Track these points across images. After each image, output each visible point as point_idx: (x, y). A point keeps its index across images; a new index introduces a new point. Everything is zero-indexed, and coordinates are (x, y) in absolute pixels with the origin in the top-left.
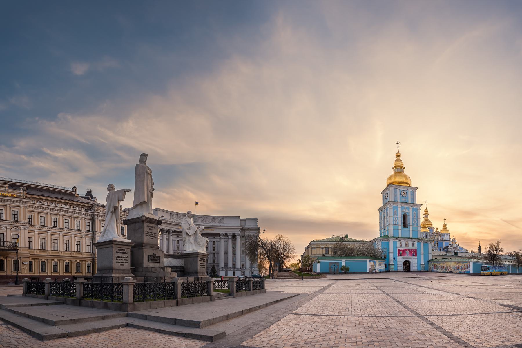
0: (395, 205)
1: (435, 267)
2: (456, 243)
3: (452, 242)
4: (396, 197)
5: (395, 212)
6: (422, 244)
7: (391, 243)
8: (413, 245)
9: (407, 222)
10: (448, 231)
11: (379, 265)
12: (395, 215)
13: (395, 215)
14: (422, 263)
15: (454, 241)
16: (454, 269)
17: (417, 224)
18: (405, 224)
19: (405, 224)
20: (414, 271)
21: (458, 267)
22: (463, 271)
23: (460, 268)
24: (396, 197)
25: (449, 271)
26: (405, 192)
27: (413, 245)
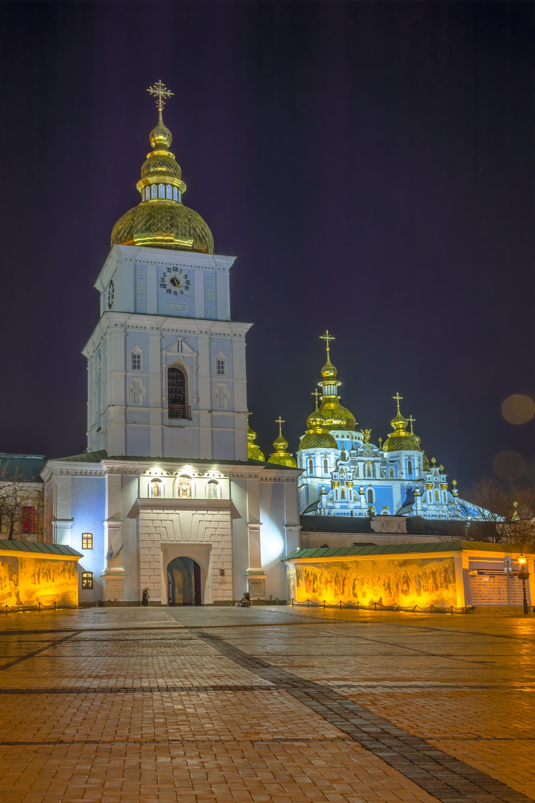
13: (136, 365)
26: (180, 278)
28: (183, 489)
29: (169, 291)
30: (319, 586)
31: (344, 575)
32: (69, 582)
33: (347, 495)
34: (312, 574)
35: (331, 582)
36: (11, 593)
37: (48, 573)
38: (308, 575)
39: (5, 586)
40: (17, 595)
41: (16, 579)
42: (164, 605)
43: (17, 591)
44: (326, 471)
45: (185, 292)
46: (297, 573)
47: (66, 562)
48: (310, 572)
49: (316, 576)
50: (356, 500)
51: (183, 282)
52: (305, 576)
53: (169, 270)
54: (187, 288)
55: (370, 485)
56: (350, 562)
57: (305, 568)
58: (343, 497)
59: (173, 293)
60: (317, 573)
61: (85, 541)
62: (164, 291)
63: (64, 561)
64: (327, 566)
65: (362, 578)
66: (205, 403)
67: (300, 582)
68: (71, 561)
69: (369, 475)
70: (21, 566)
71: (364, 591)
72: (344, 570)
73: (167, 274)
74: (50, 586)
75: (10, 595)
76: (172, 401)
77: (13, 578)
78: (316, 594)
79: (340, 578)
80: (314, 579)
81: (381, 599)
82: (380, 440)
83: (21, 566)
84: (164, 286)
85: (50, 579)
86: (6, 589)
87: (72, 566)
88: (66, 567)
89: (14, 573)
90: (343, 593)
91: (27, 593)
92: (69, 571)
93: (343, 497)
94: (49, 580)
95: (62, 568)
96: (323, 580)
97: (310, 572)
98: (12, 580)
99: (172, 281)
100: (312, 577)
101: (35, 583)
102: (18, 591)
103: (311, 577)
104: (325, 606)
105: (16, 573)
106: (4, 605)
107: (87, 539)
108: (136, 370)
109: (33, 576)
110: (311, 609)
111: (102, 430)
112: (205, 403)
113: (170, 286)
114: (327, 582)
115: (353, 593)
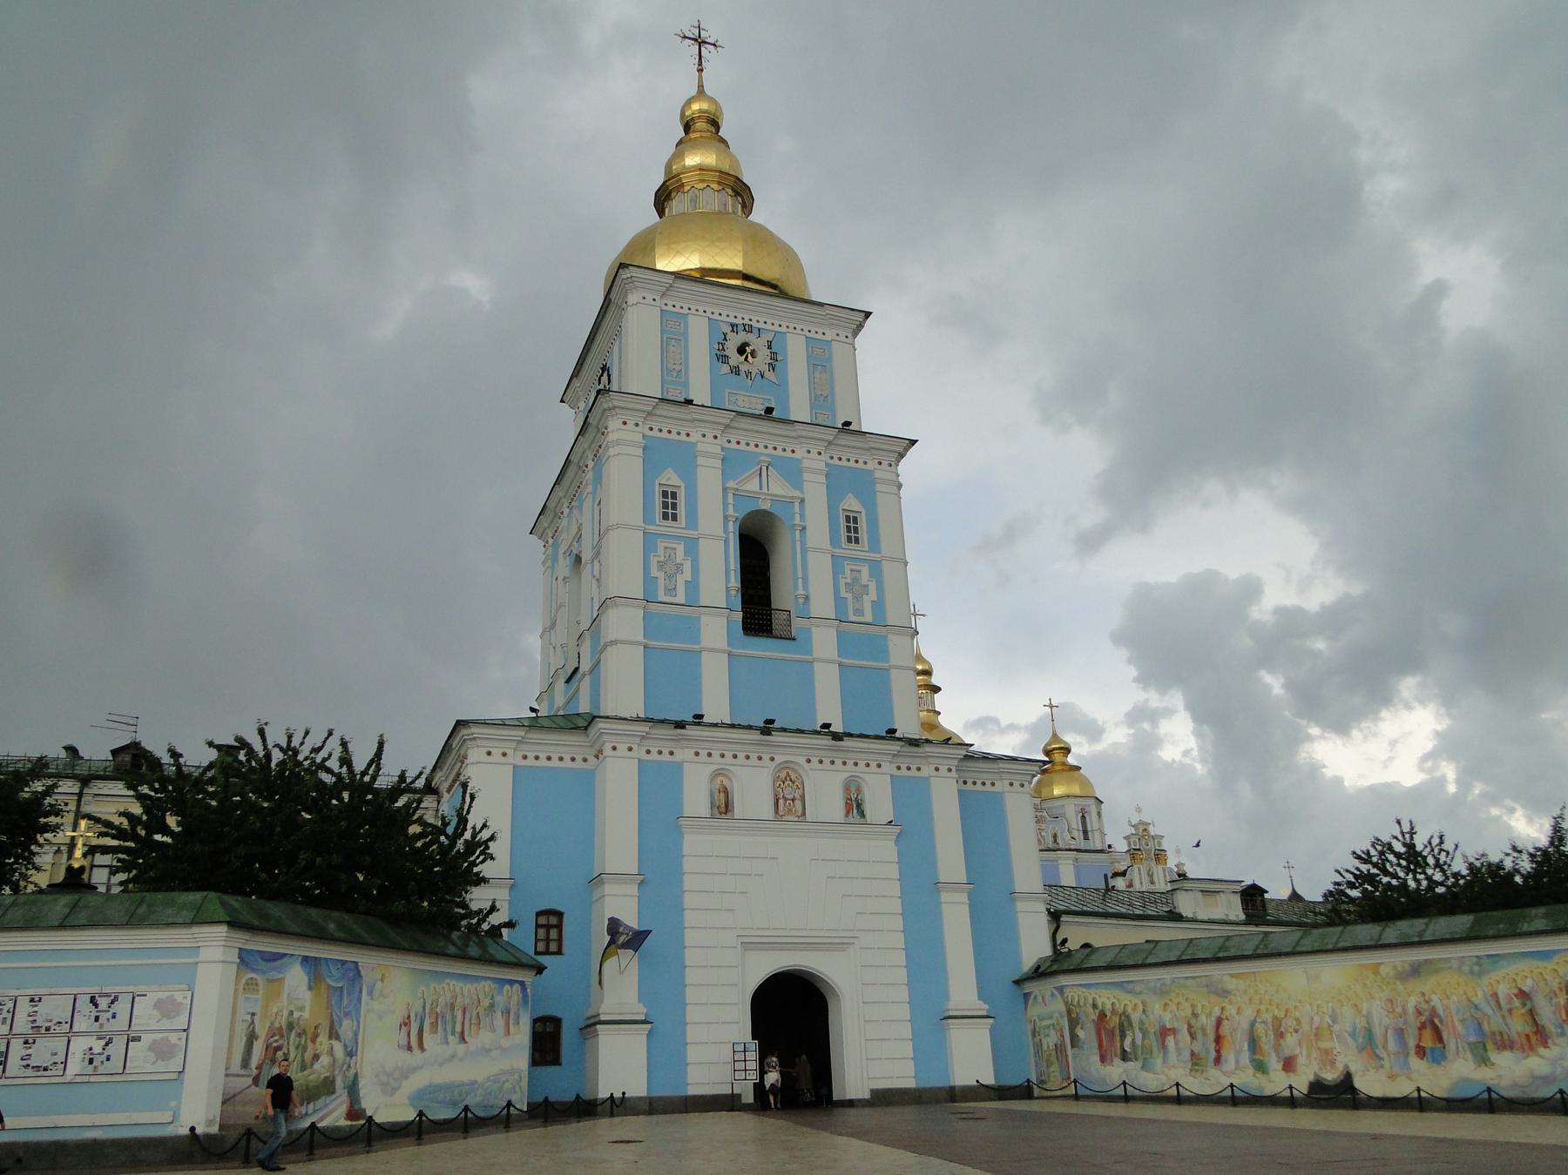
0: (671, 425)
1: (1112, 1034)
2: (1160, 856)
3: (1133, 853)
4: (673, 369)
5: (669, 498)
6: (944, 794)
7: (619, 777)
8: (855, 806)
9: (784, 594)
10: (1085, 782)
11: (414, 1033)
12: (670, 512)
13: (670, 512)
14: (963, 991)
15: (1145, 847)
16: (1368, 1044)
17: (879, 605)
18: (758, 611)
19: (758, 611)
20: (883, 1098)
21: (1432, 1025)
22: (1510, 1071)
23: (1457, 1032)
24: (673, 369)
25: (1301, 1083)
26: (758, 343)
27: (855, 806)
28: (785, 799)
29: (736, 371)
30: (1139, 1041)
31: (1217, 1012)
32: (506, 1043)
34: (1114, 1012)
36: (333, 1082)
37: (449, 1017)
38: (1102, 1015)
39: (316, 1057)
40: (353, 1089)
41: (351, 1035)
43: (352, 1071)
46: (1069, 1012)
48: (1109, 1006)
49: (1128, 1017)
51: (763, 355)
52: (1094, 1016)
53: (733, 325)
54: (772, 367)
56: (1232, 976)
57: (1091, 995)
59: (742, 373)
60: (1129, 1010)
61: (542, 932)
62: (725, 369)
63: (494, 980)
65: (1275, 1018)
66: (822, 605)
67: (1081, 1034)
68: (511, 982)
70: (370, 993)
71: (1287, 1053)
72: (1213, 997)
74: (453, 1056)
75: (327, 1087)
76: (747, 600)
77: (341, 1032)
79: (1203, 1019)
80: (1121, 1025)
81: (1348, 1077)
83: (370, 993)
84: (724, 359)
85: (453, 1033)
86: (317, 1066)
87: (515, 998)
88: (498, 999)
89: (347, 1014)
91: (384, 1079)
94: (450, 1038)
95: (486, 1003)
97: (1109, 1006)
98: (338, 1038)
99: (741, 350)
100: (1116, 1019)
101: (409, 1048)
102: (356, 1075)
105: (354, 1013)
106: (306, 1124)
107: (548, 927)
108: (670, 523)
111: (585, 666)
112: (822, 605)
113: (735, 359)
115: (1253, 1061)
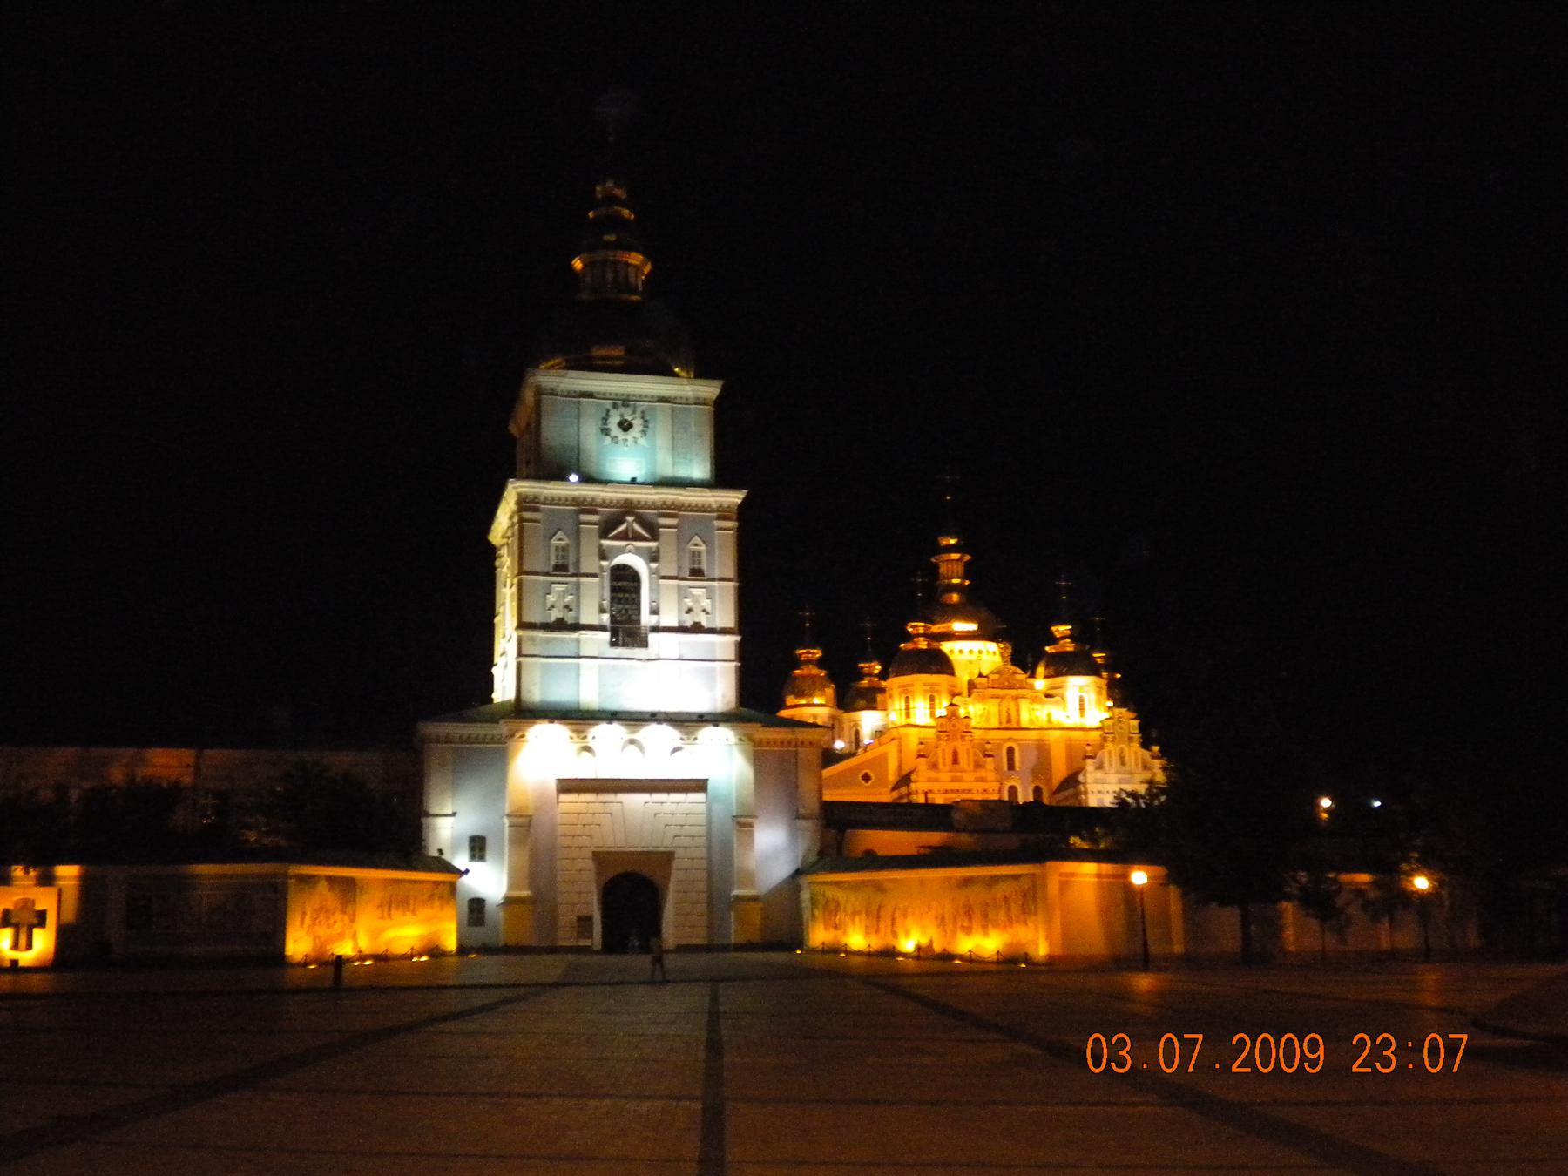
33: (962, 758)
35: (859, 913)
42: (597, 952)
44: (932, 714)
45: (642, 441)
47: (436, 883)
50: (978, 765)
55: (1009, 739)
58: (955, 761)
64: (855, 887)
67: (817, 913)
69: (1009, 721)
73: (613, 412)
78: (839, 933)
82: (1030, 659)
90: (877, 931)
92: (441, 898)
93: (955, 761)
96: (849, 909)
103: (832, 906)
104: (846, 952)
109: (381, 906)
110: (828, 957)
114: (855, 913)
